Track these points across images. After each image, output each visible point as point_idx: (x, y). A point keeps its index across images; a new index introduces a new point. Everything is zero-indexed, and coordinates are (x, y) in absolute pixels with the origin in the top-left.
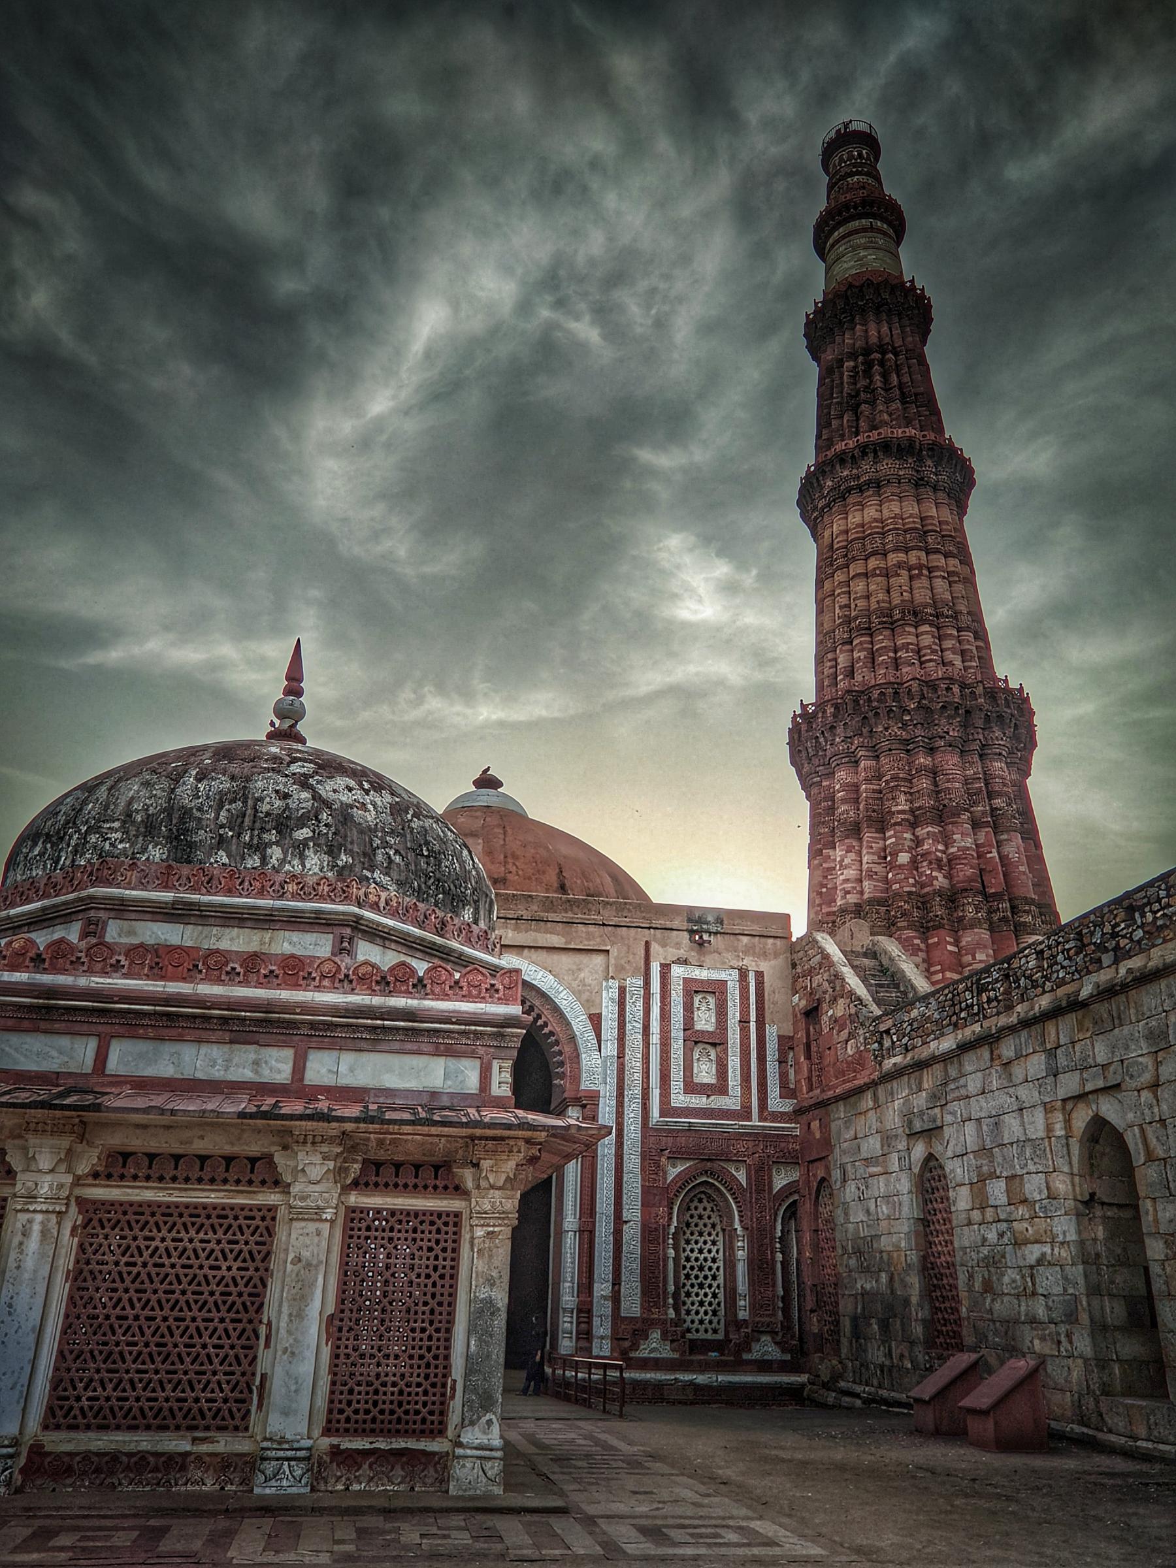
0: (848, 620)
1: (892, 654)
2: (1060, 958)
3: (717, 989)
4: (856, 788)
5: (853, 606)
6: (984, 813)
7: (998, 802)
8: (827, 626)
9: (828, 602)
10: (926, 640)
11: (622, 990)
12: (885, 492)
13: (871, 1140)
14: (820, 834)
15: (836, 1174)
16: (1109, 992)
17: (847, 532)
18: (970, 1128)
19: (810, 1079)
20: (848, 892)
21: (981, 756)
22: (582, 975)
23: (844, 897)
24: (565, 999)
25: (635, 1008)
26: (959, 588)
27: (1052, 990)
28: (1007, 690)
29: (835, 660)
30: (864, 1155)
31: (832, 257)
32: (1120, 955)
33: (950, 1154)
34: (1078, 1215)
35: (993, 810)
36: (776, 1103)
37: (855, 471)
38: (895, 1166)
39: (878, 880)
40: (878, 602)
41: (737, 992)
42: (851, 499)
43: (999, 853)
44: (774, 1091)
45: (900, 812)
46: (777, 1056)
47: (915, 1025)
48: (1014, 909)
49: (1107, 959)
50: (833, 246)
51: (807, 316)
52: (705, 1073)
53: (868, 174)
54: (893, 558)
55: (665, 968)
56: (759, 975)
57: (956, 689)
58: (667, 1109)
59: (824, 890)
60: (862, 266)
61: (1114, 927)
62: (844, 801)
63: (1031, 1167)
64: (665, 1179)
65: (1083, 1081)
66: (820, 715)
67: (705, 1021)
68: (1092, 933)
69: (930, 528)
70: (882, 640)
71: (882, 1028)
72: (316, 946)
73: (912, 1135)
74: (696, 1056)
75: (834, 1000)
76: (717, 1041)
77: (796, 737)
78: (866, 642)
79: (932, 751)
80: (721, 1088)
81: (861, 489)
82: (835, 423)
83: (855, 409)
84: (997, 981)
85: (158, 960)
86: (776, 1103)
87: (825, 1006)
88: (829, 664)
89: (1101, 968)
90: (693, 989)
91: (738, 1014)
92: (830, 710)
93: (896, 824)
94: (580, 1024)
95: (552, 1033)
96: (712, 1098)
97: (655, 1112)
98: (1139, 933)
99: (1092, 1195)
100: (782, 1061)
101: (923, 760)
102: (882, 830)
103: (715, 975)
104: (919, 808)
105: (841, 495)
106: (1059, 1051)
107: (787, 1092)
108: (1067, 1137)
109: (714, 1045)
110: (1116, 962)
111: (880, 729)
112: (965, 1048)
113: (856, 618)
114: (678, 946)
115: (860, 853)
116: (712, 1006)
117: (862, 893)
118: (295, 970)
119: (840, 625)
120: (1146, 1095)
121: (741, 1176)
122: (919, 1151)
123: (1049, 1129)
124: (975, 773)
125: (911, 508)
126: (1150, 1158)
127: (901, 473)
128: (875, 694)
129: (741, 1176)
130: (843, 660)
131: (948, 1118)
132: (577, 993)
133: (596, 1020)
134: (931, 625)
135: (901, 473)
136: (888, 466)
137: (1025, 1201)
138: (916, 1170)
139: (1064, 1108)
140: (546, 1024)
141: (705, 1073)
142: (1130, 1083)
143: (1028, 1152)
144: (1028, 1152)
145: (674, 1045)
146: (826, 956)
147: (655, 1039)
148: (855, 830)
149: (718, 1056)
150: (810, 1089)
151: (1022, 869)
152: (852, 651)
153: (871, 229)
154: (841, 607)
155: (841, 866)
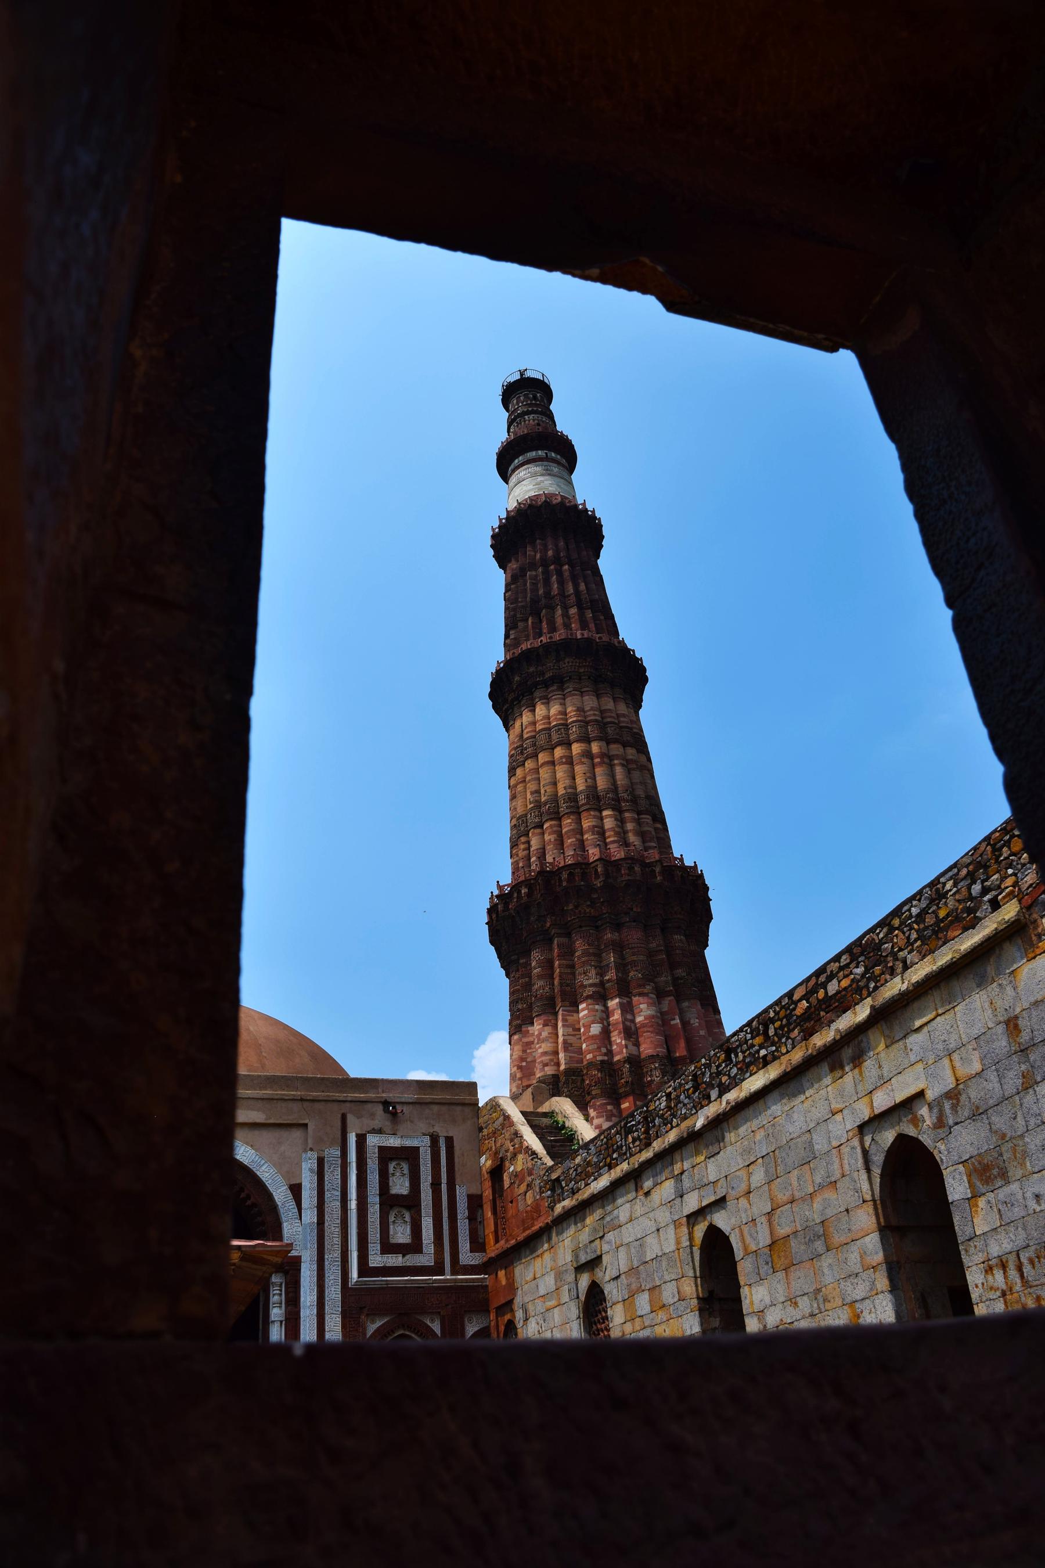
0: (538, 805)
1: (578, 836)
2: (682, 1097)
3: (410, 1155)
4: (549, 964)
5: (542, 792)
6: (667, 982)
7: (680, 972)
8: (520, 811)
9: (520, 788)
10: (609, 823)
11: (321, 1162)
12: (568, 687)
13: (546, 1278)
14: (519, 1010)
15: (519, 1314)
16: (718, 1123)
17: (534, 723)
18: (622, 1254)
19: (496, 1232)
20: (546, 1065)
21: (663, 930)
22: (282, 1148)
23: (543, 1070)
24: (266, 1173)
25: (333, 1177)
26: (636, 775)
27: (678, 1125)
28: (683, 868)
29: (528, 842)
30: (542, 1292)
31: (513, 480)
32: (724, 1090)
33: (607, 1278)
34: (701, 1310)
35: (675, 980)
36: (467, 1257)
37: (540, 668)
38: (565, 1297)
39: (574, 1052)
40: (565, 788)
41: (429, 1157)
42: (537, 694)
43: (681, 1020)
44: (464, 1245)
45: (591, 985)
46: (467, 1214)
47: (579, 1170)
49: (714, 1094)
50: (513, 471)
51: (493, 529)
52: (401, 1234)
53: (541, 413)
55: (361, 1140)
56: (449, 1140)
57: (637, 869)
58: (365, 1269)
59: (524, 1064)
60: (539, 489)
61: (718, 1067)
62: (540, 977)
63: (667, 1278)
64: (365, 1334)
65: (701, 1198)
66: (515, 895)
67: (400, 1186)
68: (703, 1074)
69: (609, 720)
71: (554, 1176)
73: (580, 1269)
74: (392, 1219)
75: (514, 1155)
76: (411, 1203)
77: (494, 916)
78: (555, 825)
79: (618, 927)
80: (415, 1246)
81: (546, 684)
82: (521, 625)
83: (536, 613)
84: (639, 1123)
86: (467, 1257)
87: (507, 1163)
88: (522, 847)
89: (710, 1102)
90: (387, 1155)
91: (430, 1178)
93: (588, 997)
94: (281, 1194)
95: (254, 1205)
96: (408, 1257)
97: (354, 1274)
98: (734, 1071)
99: (711, 1293)
100: (472, 1218)
102: (576, 1005)
103: (408, 1143)
104: (609, 981)
106: (683, 1176)
107: (477, 1245)
108: (691, 1246)
109: (408, 1208)
110: (720, 1096)
111: (571, 907)
112: (616, 1185)
113: (545, 804)
114: (372, 1116)
115: (556, 1025)
116: (406, 1171)
117: (558, 1064)
119: (532, 809)
120: (743, 1202)
121: (436, 1327)
122: (585, 1281)
123: (678, 1242)
124: (658, 946)
126: (747, 1253)
127: (582, 670)
128: (565, 875)
129: (436, 1327)
130: (535, 843)
131: (606, 1247)
132: (278, 1166)
133: (296, 1190)
134: (613, 809)
135: (582, 670)
136: (568, 664)
137: (664, 1306)
138: (582, 1298)
139: (688, 1223)
140: (248, 1197)
141: (401, 1234)
142: (733, 1194)
143: (664, 1263)
144: (664, 1263)
145: (371, 1210)
146: (507, 1118)
147: (353, 1205)
149: (412, 1217)
150: (497, 1241)
151: (702, 1033)
152: (543, 834)
153: (546, 459)
154: (532, 793)
155: (539, 1039)
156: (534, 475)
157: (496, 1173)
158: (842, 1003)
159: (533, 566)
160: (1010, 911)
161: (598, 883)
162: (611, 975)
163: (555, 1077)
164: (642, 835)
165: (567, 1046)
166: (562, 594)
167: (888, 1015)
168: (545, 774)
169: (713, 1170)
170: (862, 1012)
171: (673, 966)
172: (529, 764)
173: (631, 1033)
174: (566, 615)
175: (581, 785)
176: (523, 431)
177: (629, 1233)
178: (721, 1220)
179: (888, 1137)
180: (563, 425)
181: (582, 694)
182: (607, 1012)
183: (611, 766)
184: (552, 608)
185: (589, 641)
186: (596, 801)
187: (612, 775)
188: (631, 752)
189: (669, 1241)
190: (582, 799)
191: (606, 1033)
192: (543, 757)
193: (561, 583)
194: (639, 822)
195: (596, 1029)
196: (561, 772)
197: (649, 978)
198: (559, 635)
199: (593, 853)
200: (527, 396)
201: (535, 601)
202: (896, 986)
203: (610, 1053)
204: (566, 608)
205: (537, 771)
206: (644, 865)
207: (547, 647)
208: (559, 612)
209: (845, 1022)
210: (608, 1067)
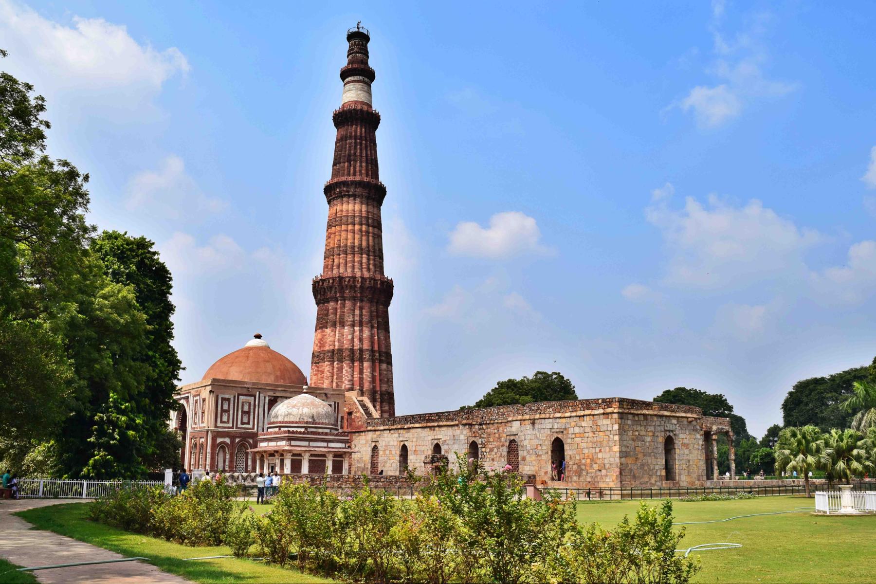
0: (339, 246)
4: (336, 309)
7: (380, 319)
8: (332, 245)
10: (364, 260)
16: (409, 428)
21: (377, 303)
26: (376, 240)
31: (347, 87)
42: (345, 199)
48: (380, 355)
54: (357, 227)
70: (350, 258)
72: (328, 431)
79: (362, 301)
81: (349, 196)
85: (313, 433)
92: (331, 281)
105: (341, 196)
107: (342, 428)
118: (326, 434)
122: (373, 444)
125: (364, 208)
136: (359, 191)
148: (334, 325)
156: (357, 89)
157: (350, 414)
158: (433, 421)
159: (351, 138)
160: (457, 422)
161: (358, 286)
162: (357, 318)
163: (333, 350)
164: (375, 265)
165: (339, 340)
166: (361, 156)
167: (439, 426)
168: (343, 234)
169: (406, 435)
170: (436, 424)
171: (378, 317)
172: (338, 228)
174: (361, 166)
175: (357, 243)
176: (355, 66)
177: (386, 439)
178: (406, 443)
179: (436, 442)
180: (372, 63)
181: (362, 203)
183: (368, 236)
184: (355, 161)
185: (368, 182)
186: (361, 250)
187: (368, 240)
188: (376, 230)
189: (395, 444)
190: (356, 249)
192: (344, 227)
193: (361, 150)
194: (374, 260)
195: (350, 337)
196: (350, 236)
197: (370, 321)
198: (358, 178)
199: (358, 274)
200: (359, 40)
201: (349, 155)
202: (441, 424)
203: (353, 346)
204: (361, 162)
205: (340, 231)
206: (375, 280)
207: (352, 182)
208: (358, 164)
209: (433, 424)
210: (352, 351)
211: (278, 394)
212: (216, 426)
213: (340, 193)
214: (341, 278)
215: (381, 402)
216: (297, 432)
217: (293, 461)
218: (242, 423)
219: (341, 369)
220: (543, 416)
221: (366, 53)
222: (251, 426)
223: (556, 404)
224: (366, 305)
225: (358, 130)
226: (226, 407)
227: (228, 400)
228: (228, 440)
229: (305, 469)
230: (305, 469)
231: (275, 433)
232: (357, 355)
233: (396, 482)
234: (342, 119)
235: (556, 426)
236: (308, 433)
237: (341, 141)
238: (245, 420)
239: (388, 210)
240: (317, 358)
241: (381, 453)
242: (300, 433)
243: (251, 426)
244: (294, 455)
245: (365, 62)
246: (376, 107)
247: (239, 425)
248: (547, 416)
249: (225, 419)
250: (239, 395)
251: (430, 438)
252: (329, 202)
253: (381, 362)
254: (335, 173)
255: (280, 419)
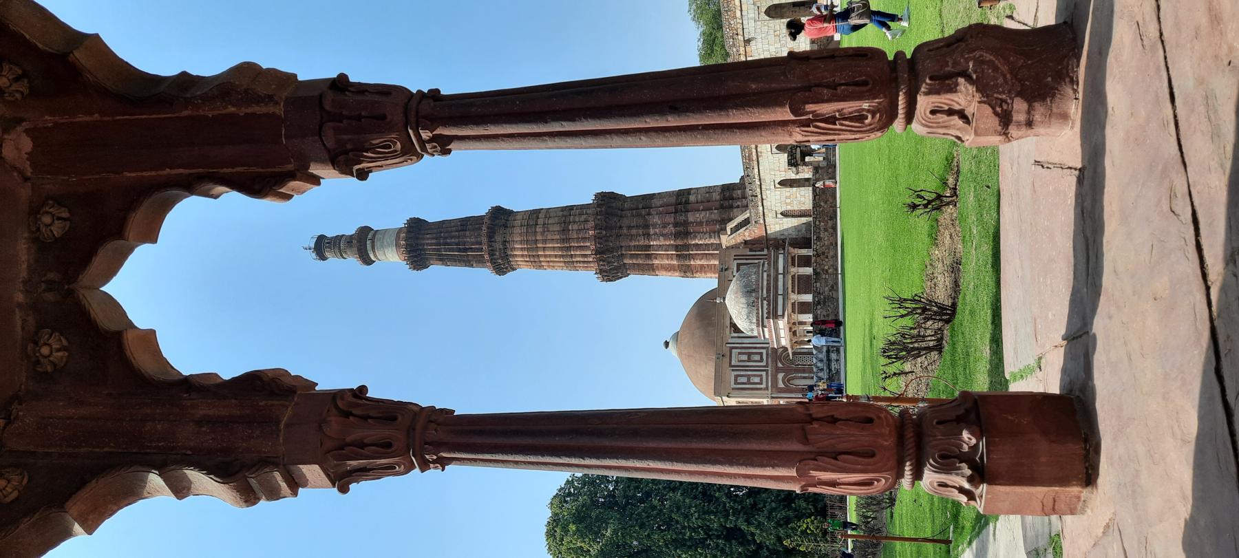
10: (576, 227)
79: (621, 227)
101: (625, 231)
105: (506, 257)
118: (769, 276)
125: (517, 230)
136: (498, 238)
162: (641, 232)
173: (665, 225)
180: (351, 230)
182: (655, 234)
191: (663, 235)
198: (484, 239)
200: (323, 246)
207: (490, 246)
211: (728, 324)
212: (767, 388)
213: (502, 258)
214: (597, 252)
215: (733, 199)
216: (768, 309)
217: (801, 312)
218: (761, 360)
219: (698, 246)
220: (740, 32)
221: (338, 239)
222: (764, 351)
223: (725, 16)
224: (625, 222)
225: (428, 243)
226: (744, 380)
227: (736, 377)
228: (781, 376)
229: (808, 298)
230: (808, 298)
231: (770, 331)
232: (681, 229)
233: (820, 206)
234: (418, 260)
235: (752, 15)
236: (768, 296)
237: (444, 260)
238: (757, 357)
239: (518, 203)
240: (687, 271)
241: (789, 208)
242: (769, 305)
243: (764, 351)
244: (793, 311)
245: (350, 240)
246: (401, 223)
247: (764, 364)
248: (740, 26)
249: (757, 380)
250: (731, 366)
251: (770, 156)
252: (514, 269)
253: (687, 202)
254: (480, 261)
255: (754, 327)
